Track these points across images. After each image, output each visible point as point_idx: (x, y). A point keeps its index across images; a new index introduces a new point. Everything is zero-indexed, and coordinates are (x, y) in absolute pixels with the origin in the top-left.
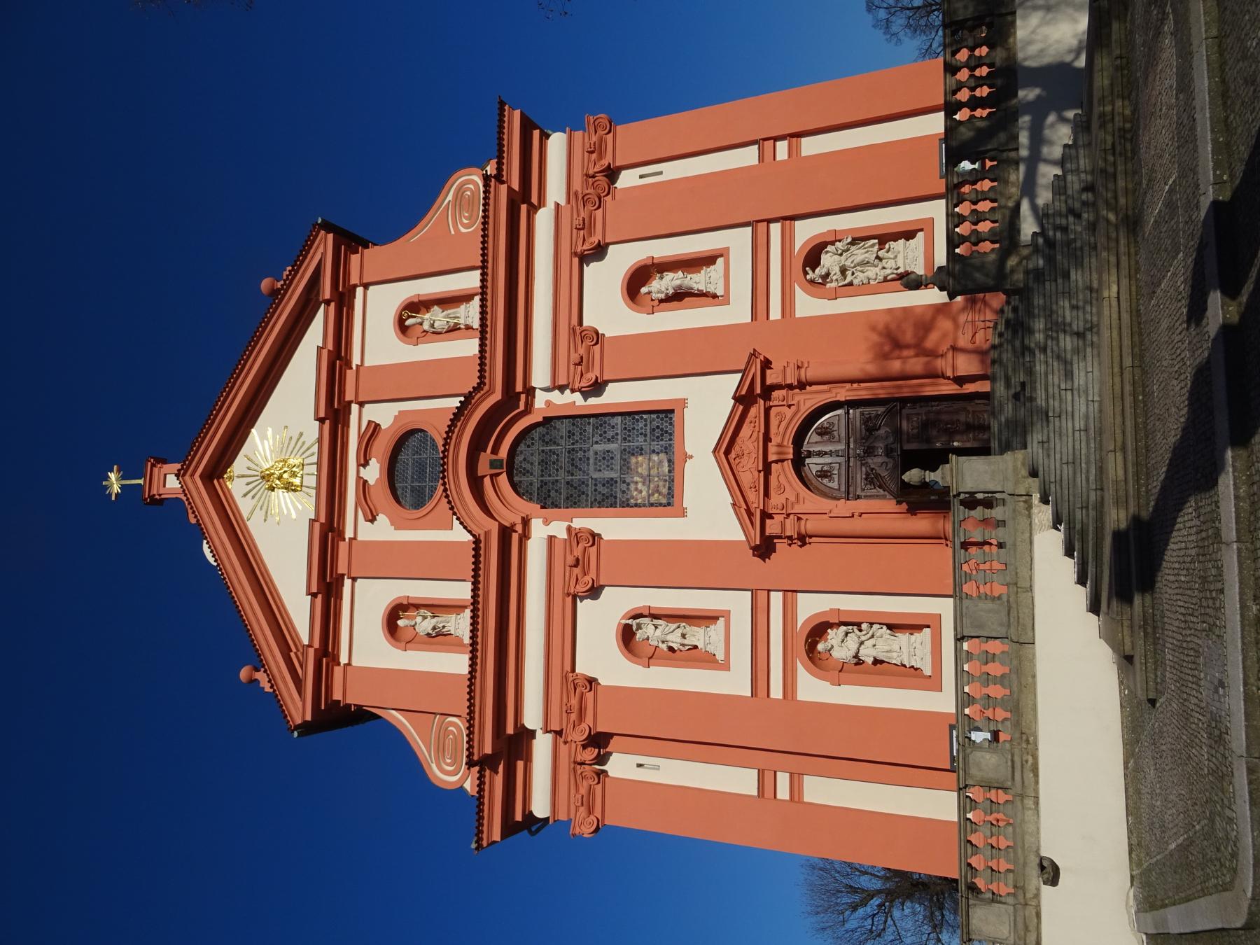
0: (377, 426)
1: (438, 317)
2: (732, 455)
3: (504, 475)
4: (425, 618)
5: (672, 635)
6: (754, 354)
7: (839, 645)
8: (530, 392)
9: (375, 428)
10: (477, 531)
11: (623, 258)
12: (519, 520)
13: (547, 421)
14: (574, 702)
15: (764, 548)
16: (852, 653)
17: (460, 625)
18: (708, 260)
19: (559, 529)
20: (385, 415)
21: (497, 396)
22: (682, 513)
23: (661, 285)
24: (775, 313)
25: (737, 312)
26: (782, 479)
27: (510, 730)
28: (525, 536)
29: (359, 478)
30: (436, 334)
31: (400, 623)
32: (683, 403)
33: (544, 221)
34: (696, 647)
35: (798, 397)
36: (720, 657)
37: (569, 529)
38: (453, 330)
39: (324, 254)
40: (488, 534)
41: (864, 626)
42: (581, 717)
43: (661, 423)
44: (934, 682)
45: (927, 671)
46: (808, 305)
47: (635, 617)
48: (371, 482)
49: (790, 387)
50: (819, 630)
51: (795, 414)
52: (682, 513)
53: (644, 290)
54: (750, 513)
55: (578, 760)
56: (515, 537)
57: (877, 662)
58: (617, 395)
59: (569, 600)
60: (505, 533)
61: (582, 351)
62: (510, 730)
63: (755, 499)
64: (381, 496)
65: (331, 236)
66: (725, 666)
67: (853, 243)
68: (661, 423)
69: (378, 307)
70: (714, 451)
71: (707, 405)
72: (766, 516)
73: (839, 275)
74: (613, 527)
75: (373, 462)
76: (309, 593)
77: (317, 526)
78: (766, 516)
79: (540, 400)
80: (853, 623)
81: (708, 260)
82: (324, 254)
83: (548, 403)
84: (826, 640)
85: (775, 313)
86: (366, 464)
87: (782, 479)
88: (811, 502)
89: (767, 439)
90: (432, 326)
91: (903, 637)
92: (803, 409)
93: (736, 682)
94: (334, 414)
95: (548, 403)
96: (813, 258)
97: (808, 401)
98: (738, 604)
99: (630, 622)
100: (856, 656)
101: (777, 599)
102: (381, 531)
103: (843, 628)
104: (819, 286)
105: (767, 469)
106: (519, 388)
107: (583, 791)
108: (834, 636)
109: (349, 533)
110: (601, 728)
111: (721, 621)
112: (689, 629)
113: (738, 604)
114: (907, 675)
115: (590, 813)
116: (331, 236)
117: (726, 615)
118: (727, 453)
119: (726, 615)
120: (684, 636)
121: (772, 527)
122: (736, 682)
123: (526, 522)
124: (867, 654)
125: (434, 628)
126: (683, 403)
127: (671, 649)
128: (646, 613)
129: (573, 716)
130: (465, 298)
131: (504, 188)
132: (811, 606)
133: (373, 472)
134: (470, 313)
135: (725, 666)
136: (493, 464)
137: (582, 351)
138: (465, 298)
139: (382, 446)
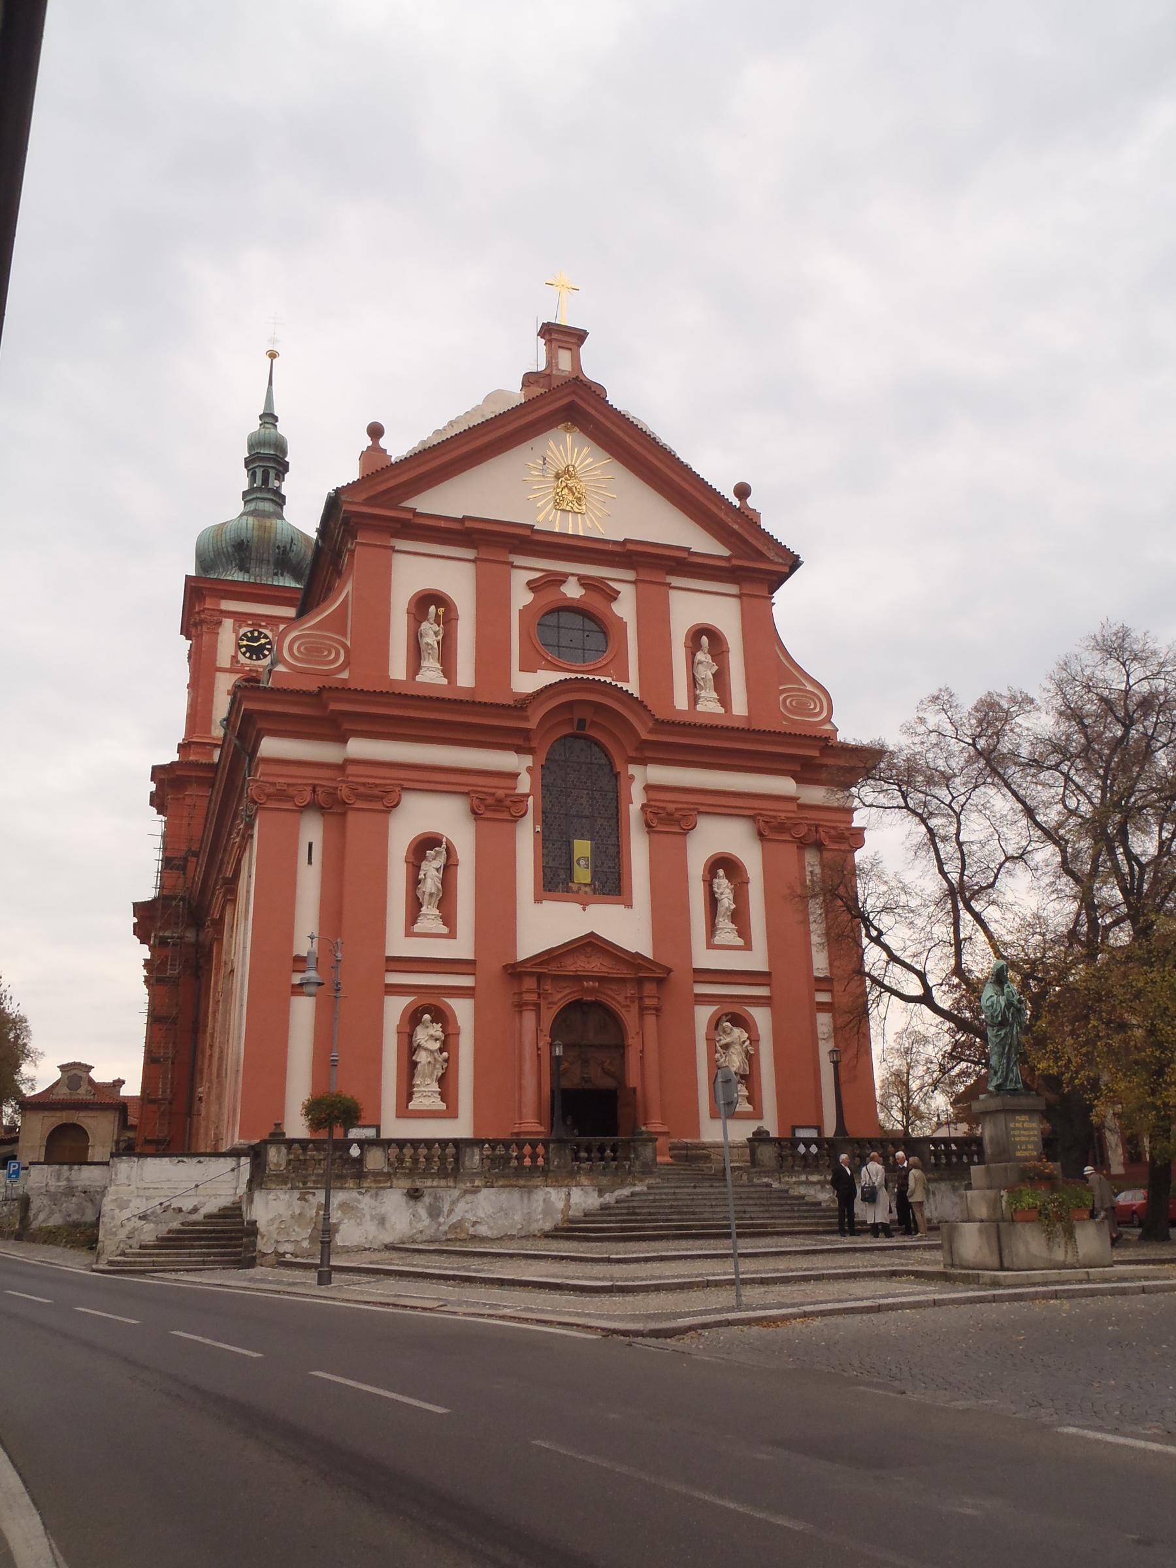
0: (615, 599)
2: (589, 949)
3: (567, 730)
4: (436, 634)
6: (669, 971)
7: (428, 1035)
8: (643, 762)
9: (613, 596)
10: (529, 712)
11: (751, 857)
12: (534, 744)
13: (616, 776)
14: (376, 792)
15: (515, 972)
16: (423, 1043)
17: (431, 674)
18: (743, 931)
19: (524, 784)
20: (625, 608)
21: (644, 736)
22: (538, 900)
23: (723, 885)
24: (700, 989)
25: (704, 958)
26: (567, 991)
27: (347, 726)
28: (519, 750)
29: (566, 575)
30: (692, 664)
31: (432, 608)
32: (629, 905)
33: (784, 785)
34: (421, 906)
35: (635, 1009)
36: (417, 928)
37: (528, 795)
38: (693, 683)
39: (772, 562)
40: (527, 719)
41: (445, 1054)
42: (360, 797)
44: (404, 1112)
45: (412, 1106)
46: (704, 1015)
47: (447, 850)
48: (563, 589)
49: (641, 999)
50: (441, 1016)
51: (618, 1002)
52: (538, 900)
53: (721, 872)
54: (540, 964)
55: (319, 790)
56: (520, 742)
57: (414, 1064)
59: (466, 789)
60: (526, 733)
61: (677, 815)
62: (347, 726)
63: (553, 969)
64: (549, 598)
65: (787, 570)
66: (409, 933)
67: (747, 1052)
68: (611, 884)
69: (719, 610)
70: (592, 933)
71: (627, 927)
72: (540, 977)
73: (723, 1042)
75: (583, 592)
76: (465, 518)
77: (528, 532)
78: (540, 977)
79: (633, 770)
80: (448, 1043)
81: (743, 931)
82: (772, 562)
83: (632, 778)
84: (432, 1022)
85: (700, 989)
86: (581, 585)
87: (567, 991)
88: (549, 1016)
89: (600, 979)
90: (700, 663)
91: (435, 1087)
92: (623, 1010)
94: (629, 555)
95: (632, 778)
96: (739, 1021)
97: (630, 1018)
98: (462, 947)
99: (444, 846)
100: (419, 1046)
101: (466, 981)
102: (521, 597)
103: (439, 1034)
104: (715, 1024)
105: (578, 978)
106: (648, 754)
107: (291, 791)
108: (436, 1030)
109: (519, 560)
110: (351, 816)
111: (444, 930)
112: (435, 900)
114: (407, 1092)
115: (269, 796)
116: (787, 570)
117: (452, 935)
118: (589, 944)
119: (452, 935)
120: (431, 895)
121: (530, 983)
123: (529, 751)
124: (422, 1057)
125: (428, 644)
126: (629, 905)
127: (419, 882)
128: (451, 862)
129: (362, 790)
130: (724, 698)
131: (816, 753)
132: (463, 1010)
133: (572, 591)
135: (409, 933)
136: (582, 723)
137: (677, 815)
138: (724, 698)
139: (596, 603)
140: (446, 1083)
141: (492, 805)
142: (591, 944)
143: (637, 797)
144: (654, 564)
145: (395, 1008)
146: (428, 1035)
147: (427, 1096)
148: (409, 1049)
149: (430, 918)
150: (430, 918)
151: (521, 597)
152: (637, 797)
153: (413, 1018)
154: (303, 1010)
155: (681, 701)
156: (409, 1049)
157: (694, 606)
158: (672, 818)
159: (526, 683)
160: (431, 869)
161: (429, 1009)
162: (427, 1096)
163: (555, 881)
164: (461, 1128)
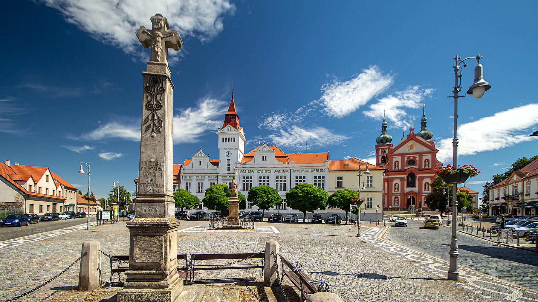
1: (427, 163)
5: (397, 187)
20: (417, 159)
38: (425, 165)
43: (414, 186)
50: (398, 198)
58: (417, 182)
68: (414, 186)
71: (416, 189)
74: (406, 182)
80: (398, 200)
93: (393, 192)
102: (406, 160)
113: (399, 192)
122: (393, 192)
130: (429, 166)
132: (399, 197)
133: (411, 158)
134: (427, 167)
140: (398, 203)
141: (402, 179)
142: (411, 191)
143: (417, 178)
144: (421, 154)
145: (393, 197)
146: (396, 199)
147: (396, 204)
148: (395, 201)
149: (396, 190)
150: (396, 190)
151: (406, 160)
152: (417, 178)
153: (395, 198)
154: (386, 197)
155: (423, 167)
156: (395, 201)
157: (425, 157)
158: (421, 179)
159: (406, 168)
160: (397, 186)
161: (397, 197)
162: (396, 204)
163: (408, 186)
164: (399, 206)
